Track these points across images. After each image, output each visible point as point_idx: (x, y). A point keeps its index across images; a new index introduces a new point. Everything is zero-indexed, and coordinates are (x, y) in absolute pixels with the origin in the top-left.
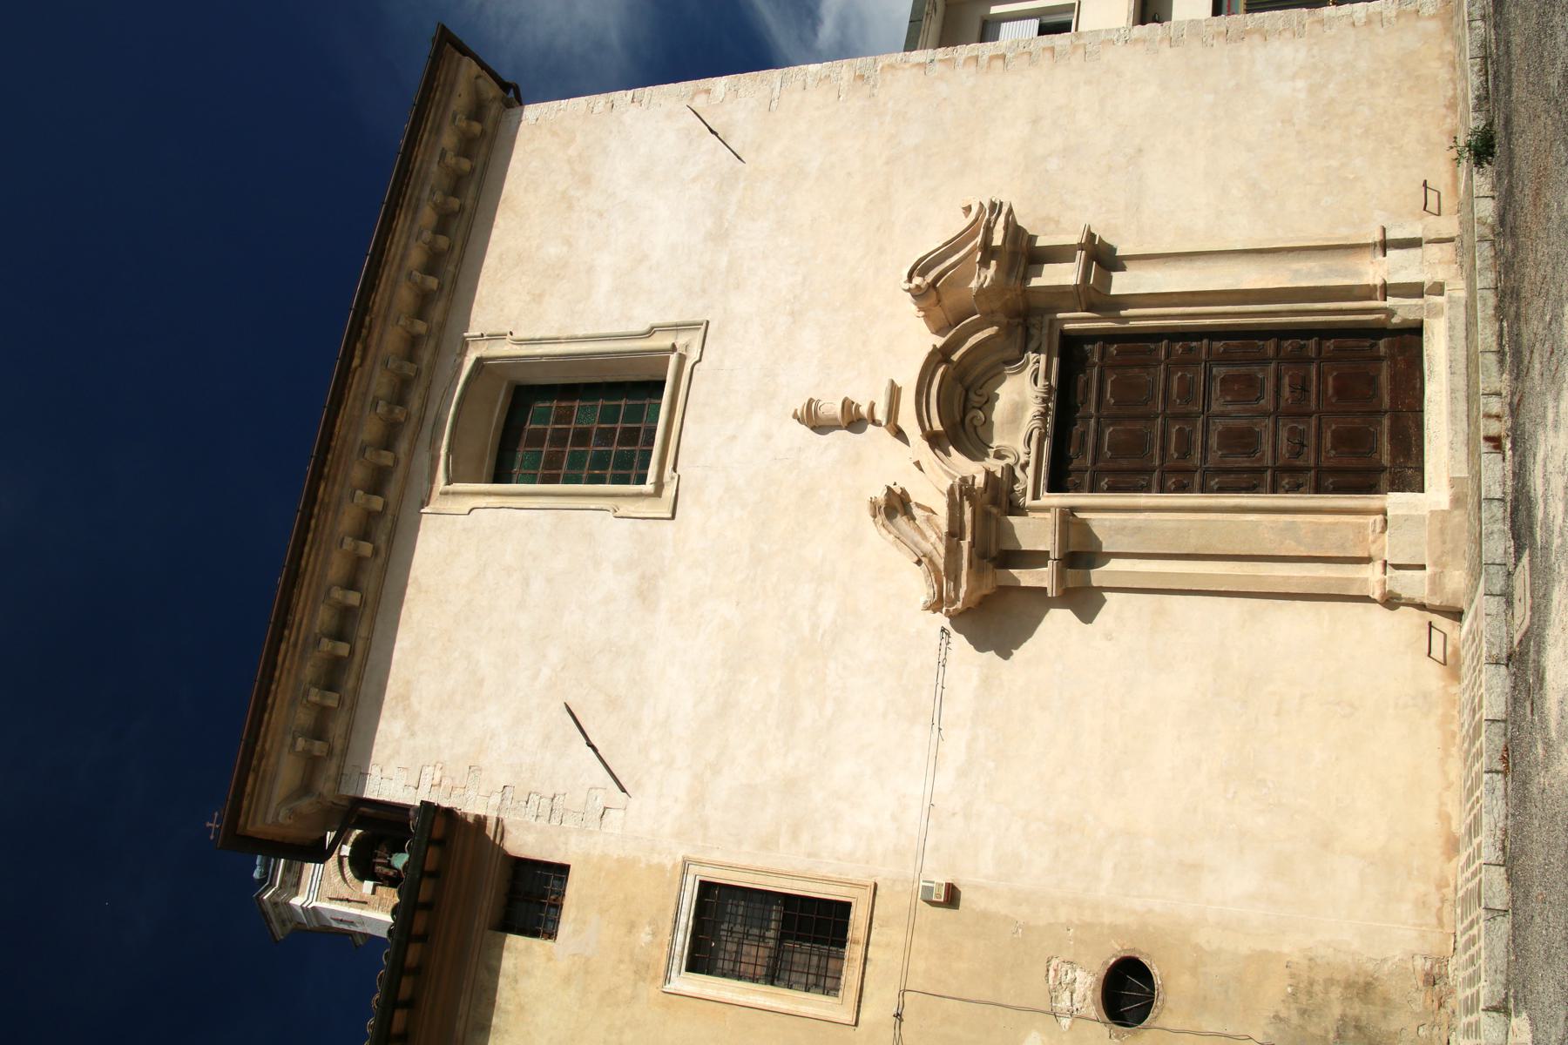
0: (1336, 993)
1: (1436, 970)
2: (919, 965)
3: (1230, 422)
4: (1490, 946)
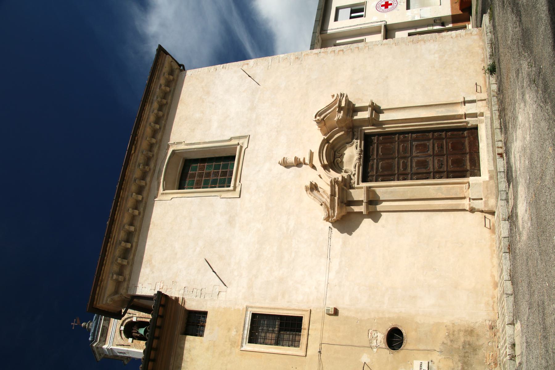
0: (462, 334)
1: (493, 324)
2: (326, 335)
3: (419, 159)
4: (508, 305)
